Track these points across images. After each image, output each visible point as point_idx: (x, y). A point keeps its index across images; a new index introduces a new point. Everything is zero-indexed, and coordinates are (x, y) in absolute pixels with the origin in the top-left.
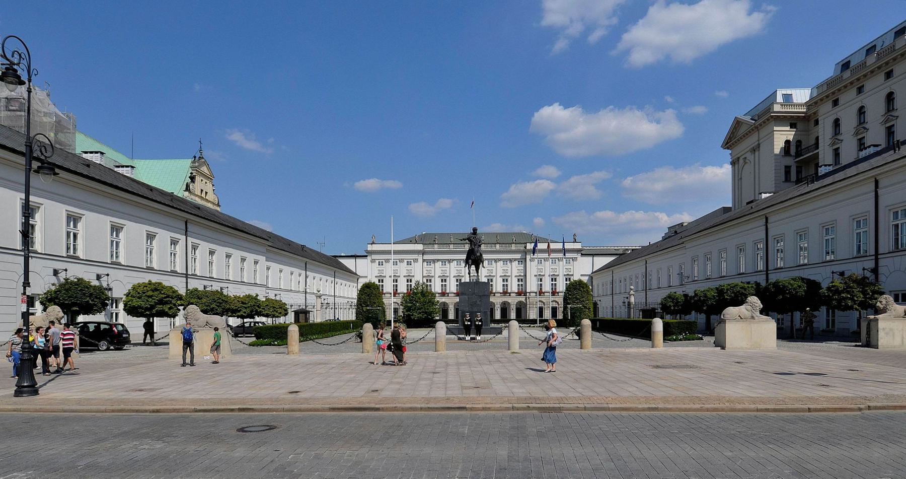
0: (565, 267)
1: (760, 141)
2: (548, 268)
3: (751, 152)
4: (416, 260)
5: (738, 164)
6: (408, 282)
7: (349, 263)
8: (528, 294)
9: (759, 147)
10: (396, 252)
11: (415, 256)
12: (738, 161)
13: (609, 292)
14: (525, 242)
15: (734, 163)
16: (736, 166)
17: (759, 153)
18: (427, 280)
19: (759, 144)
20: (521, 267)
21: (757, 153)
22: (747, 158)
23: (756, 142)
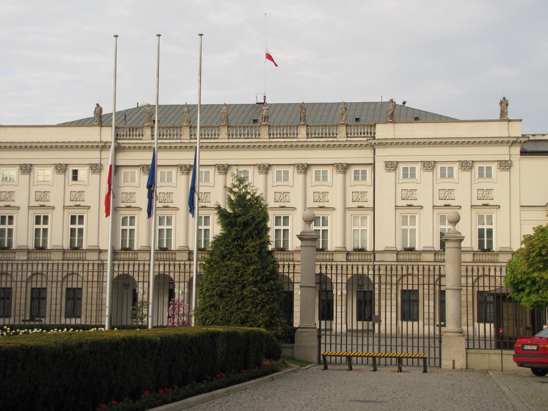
0: (476, 187)
4: (96, 168)
6: (38, 222)
8: (378, 257)
11: (93, 156)
20: (365, 187)
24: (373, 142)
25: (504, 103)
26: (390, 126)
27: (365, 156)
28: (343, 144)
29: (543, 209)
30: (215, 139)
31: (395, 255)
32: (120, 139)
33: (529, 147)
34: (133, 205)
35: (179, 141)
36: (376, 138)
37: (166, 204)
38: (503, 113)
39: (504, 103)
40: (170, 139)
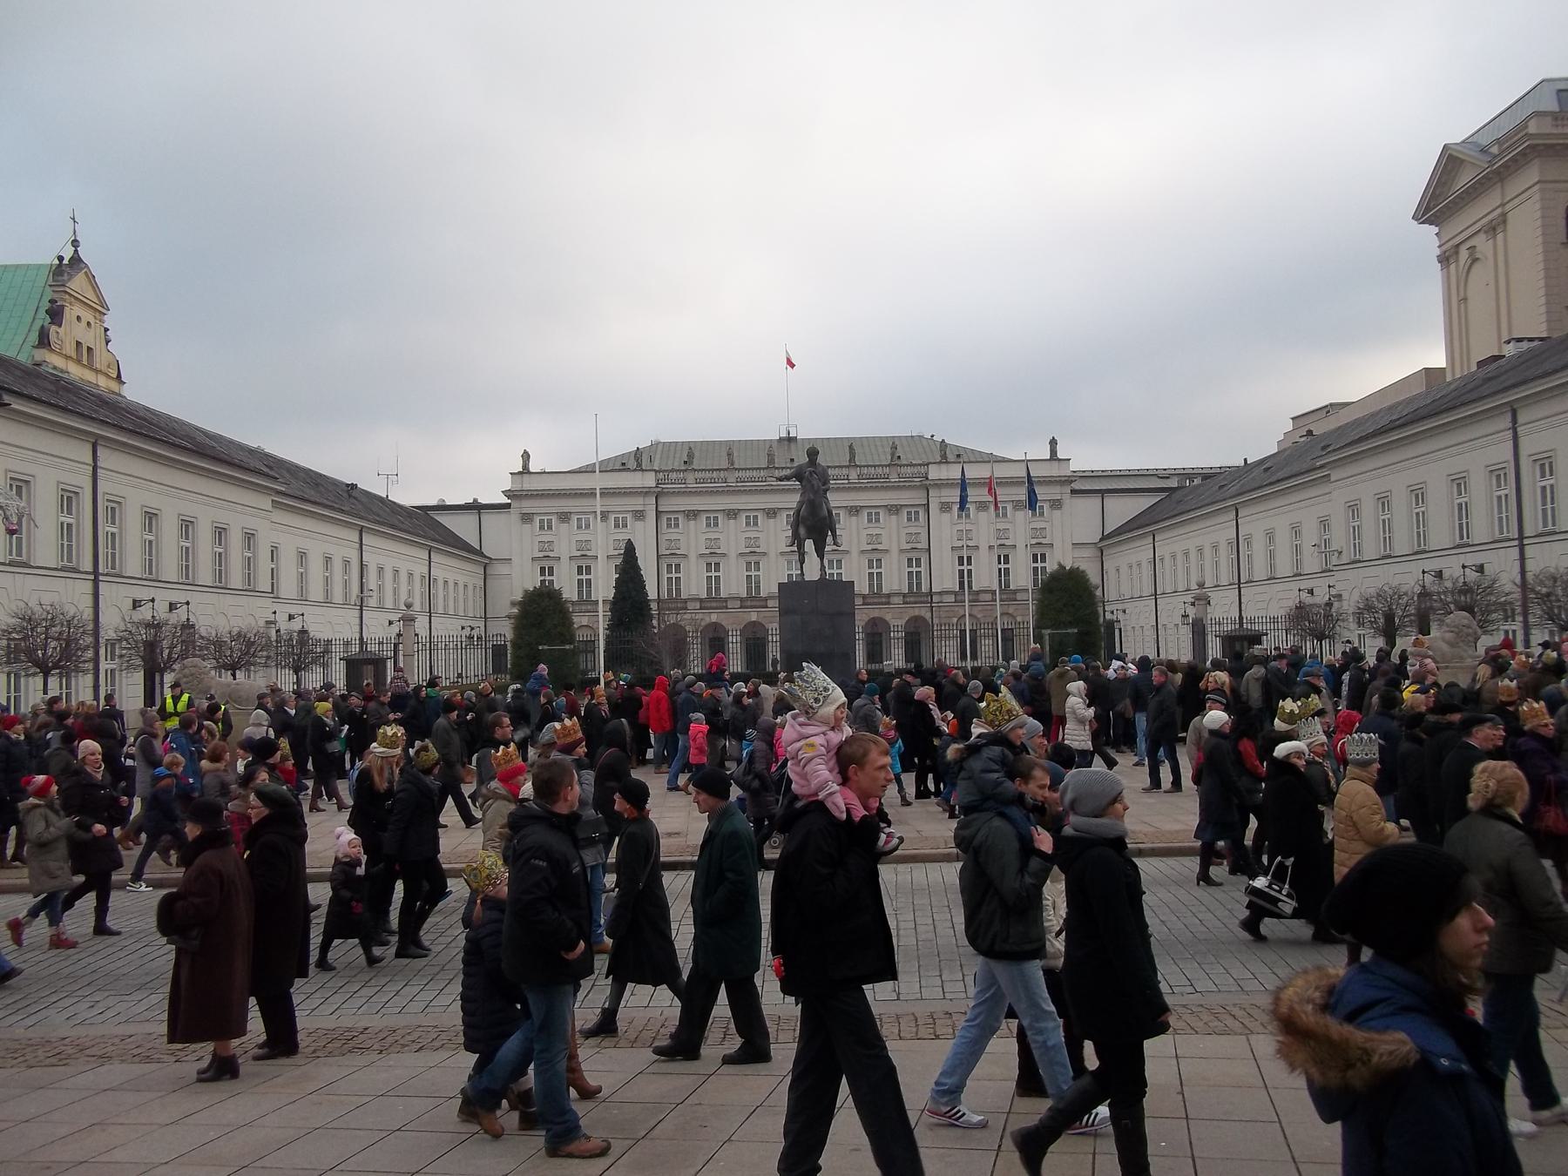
1: (1508, 207)
2: (983, 527)
3: (1486, 232)
4: (639, 515)
5: (1457, 261)
7: (463, 527)
8: (935, 599)
9: (1505, 222)
10: (606, 493)
11: (637, 503)
12: (1457, 253)
13: (1148, 590)
14: (926, 461)
15: (1447, 259)
16: (1453, 267)
17: (1505, 240)
18: (669, 566)
19: (1504, 215)
21: (1500, 237)
22: (1478, 249)
23: (1499, 207)
24: (928, 482)
25: (1053, 443)
26: (944, 467)
27: (916, 497)
28: (896, 484)
29: (1093, 546)
30: (762, 481)
31: (953, 596)
32: (661, 484)
33: (1077, 486)
34: (678, 552)
35: (725, 485)
36: (930, 478)
37: (713, 551)
38: (1053, 452)
39: (1053, 443)
40: (715, 483)
